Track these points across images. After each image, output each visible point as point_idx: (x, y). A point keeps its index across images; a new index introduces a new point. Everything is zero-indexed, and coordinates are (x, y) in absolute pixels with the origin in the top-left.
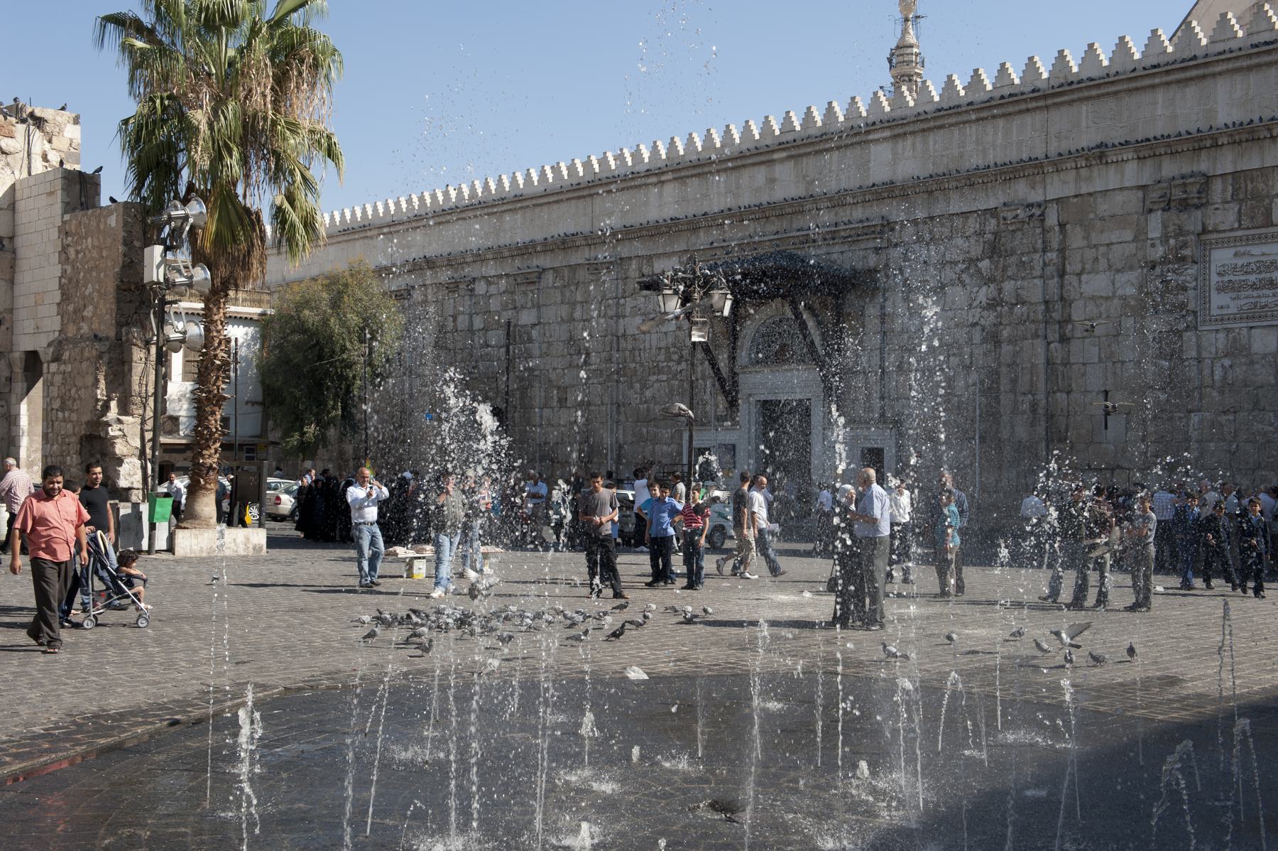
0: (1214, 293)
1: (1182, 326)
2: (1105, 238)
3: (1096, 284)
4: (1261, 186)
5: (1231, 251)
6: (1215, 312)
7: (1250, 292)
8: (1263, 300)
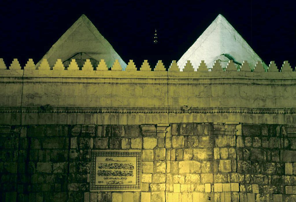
0: (97, 175)
1: (84, 189)
2: (50, 146)
3: (45, 167)
4: (117, 132)
5: (105, 158)
6: (97, 184)
7: (112, 176)
8: (117, 180)
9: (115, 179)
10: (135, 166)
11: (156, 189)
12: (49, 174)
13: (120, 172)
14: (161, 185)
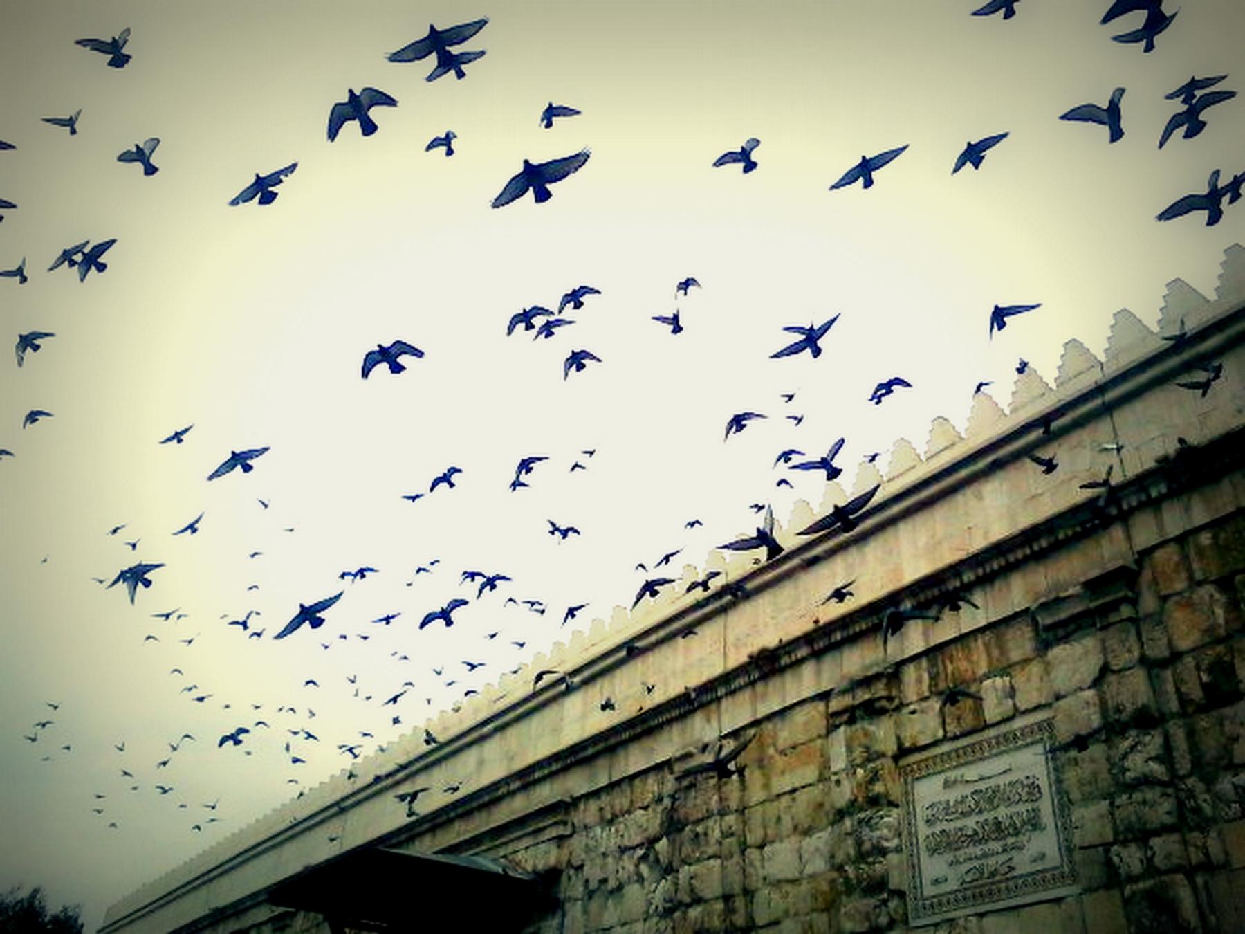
0: (924, 856)
5: (938, 781)
6: (929, 891)
8: (991, 861)
9: (985, 855)
10: (1043, 783)
11: (1137, 868)
12: (794, 882)
13: (998, 824)
14: (1155, 842)
